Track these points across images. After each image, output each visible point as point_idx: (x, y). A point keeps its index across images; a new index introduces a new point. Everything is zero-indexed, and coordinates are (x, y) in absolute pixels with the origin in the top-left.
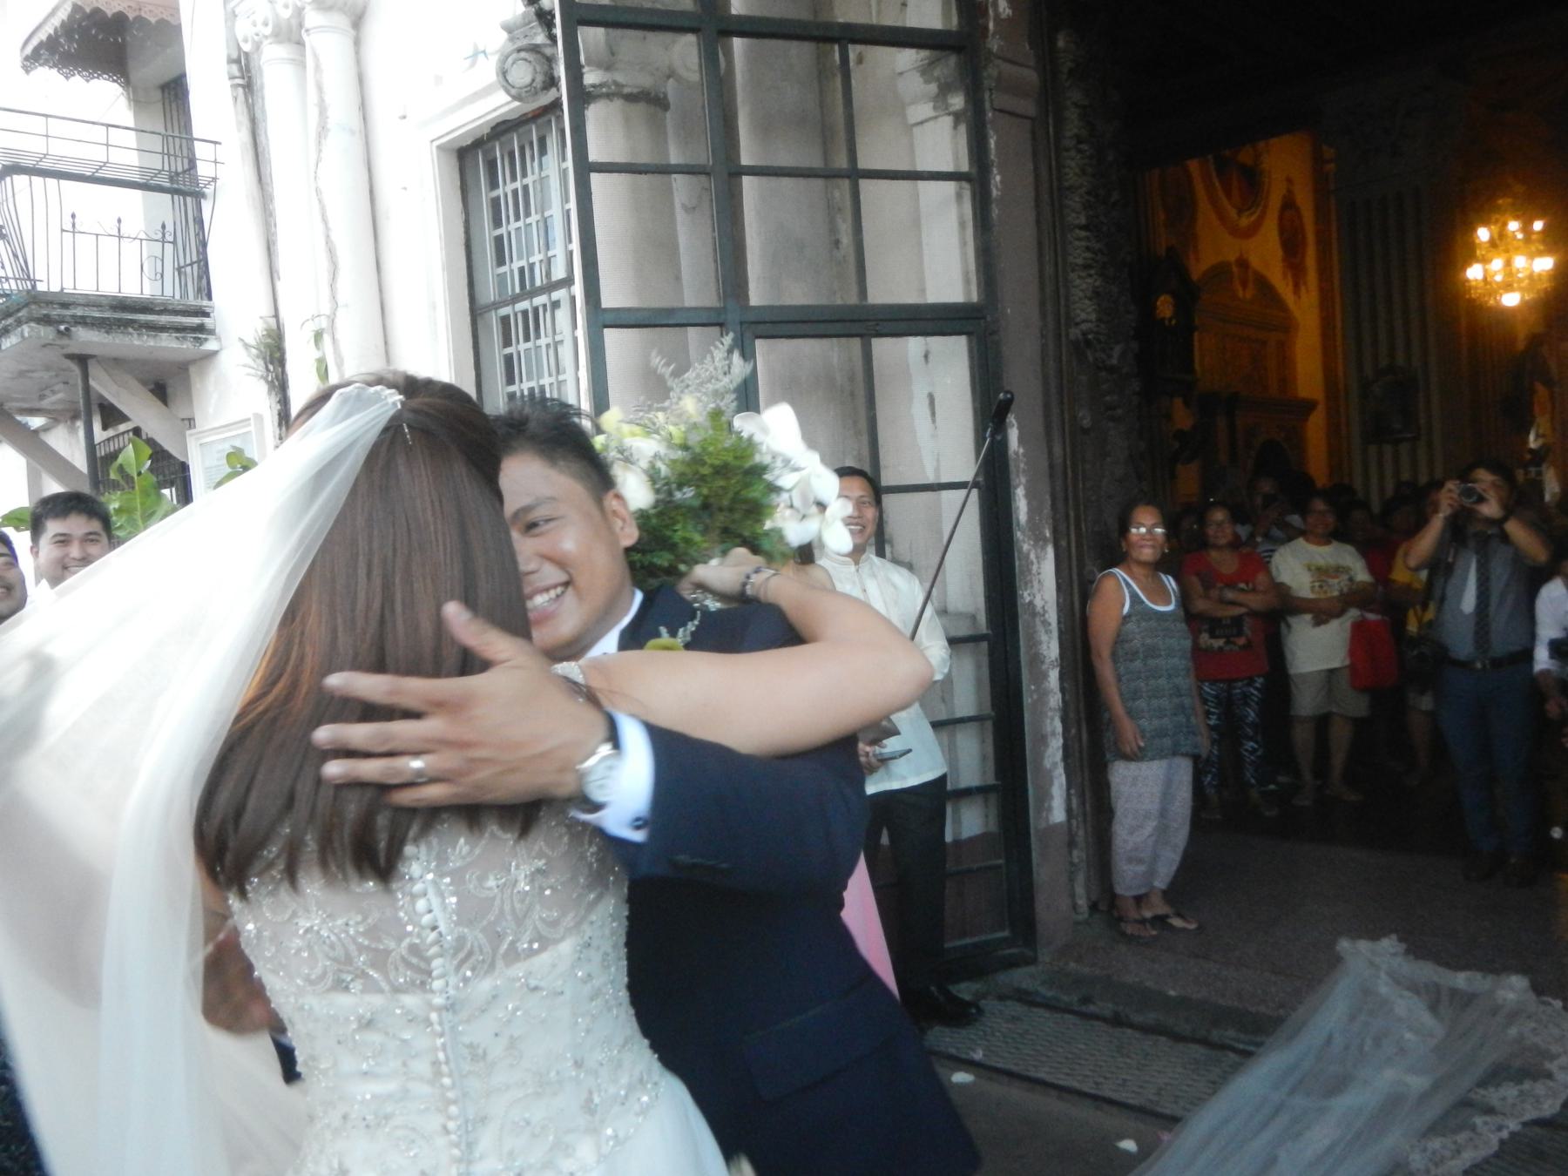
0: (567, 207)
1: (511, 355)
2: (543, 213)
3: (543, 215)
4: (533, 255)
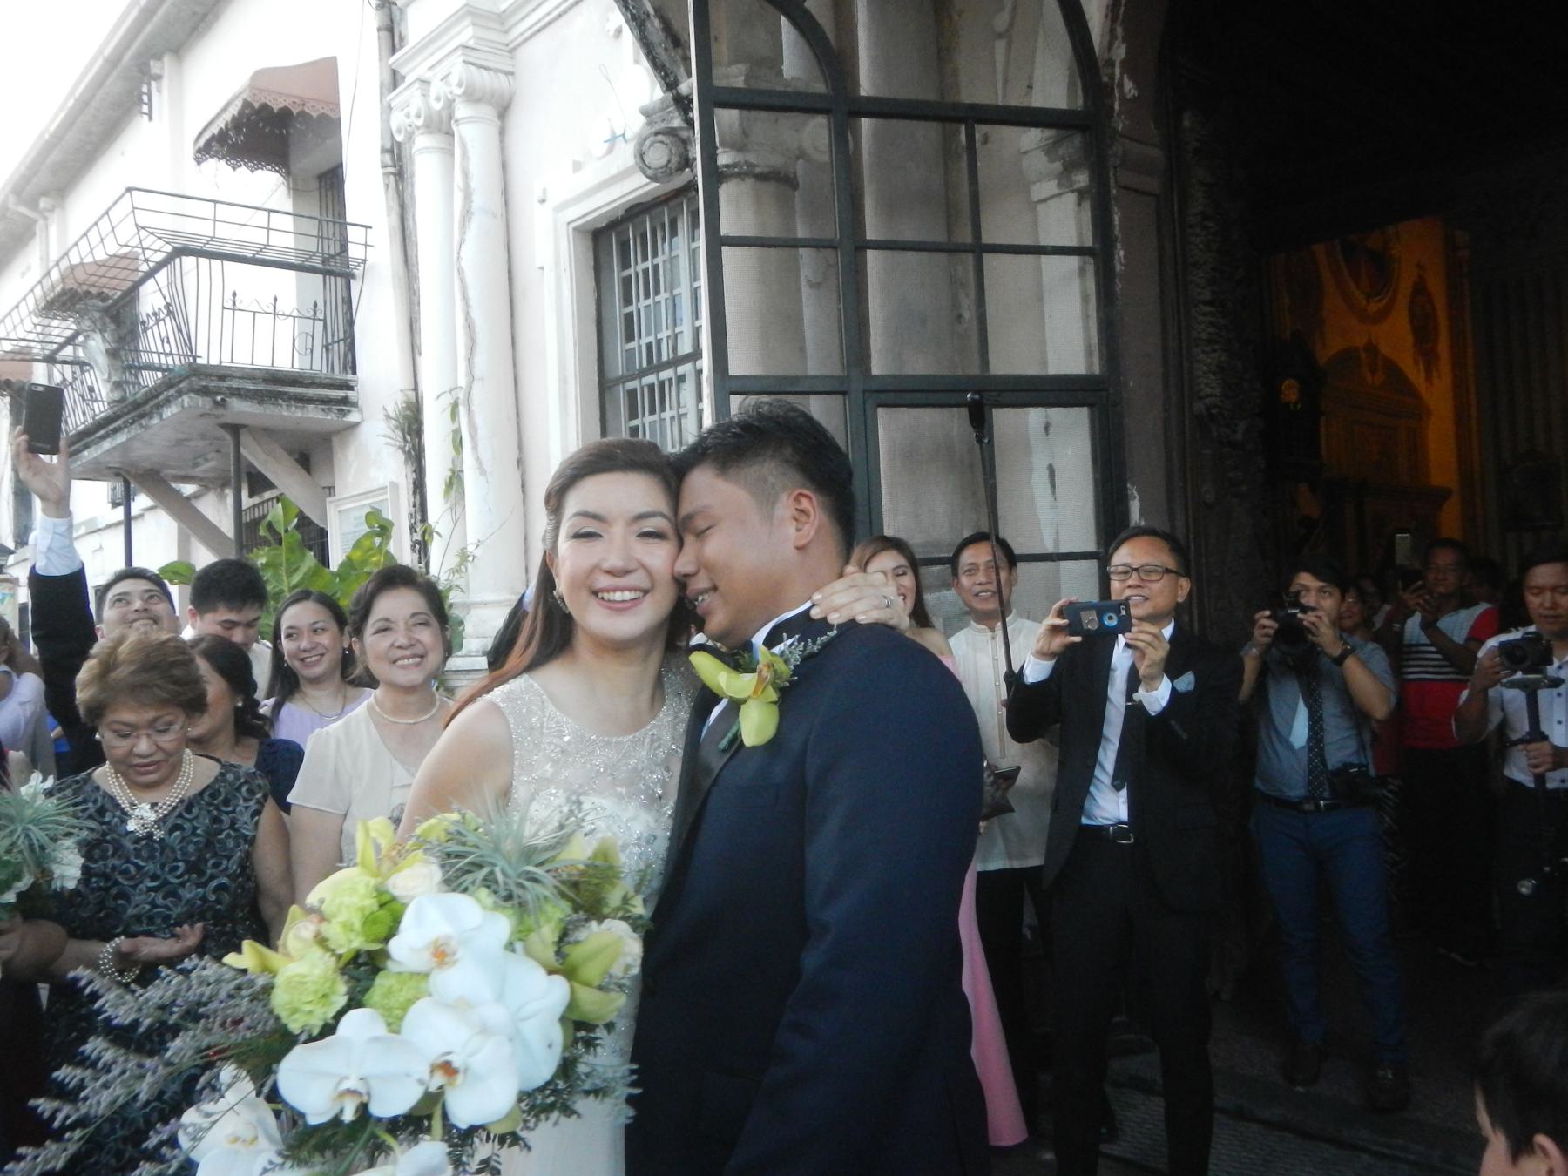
0: (696, 285)
1: (637, 427)
2: (672, 292)
3: (672, 292)
4: (661, 330)
